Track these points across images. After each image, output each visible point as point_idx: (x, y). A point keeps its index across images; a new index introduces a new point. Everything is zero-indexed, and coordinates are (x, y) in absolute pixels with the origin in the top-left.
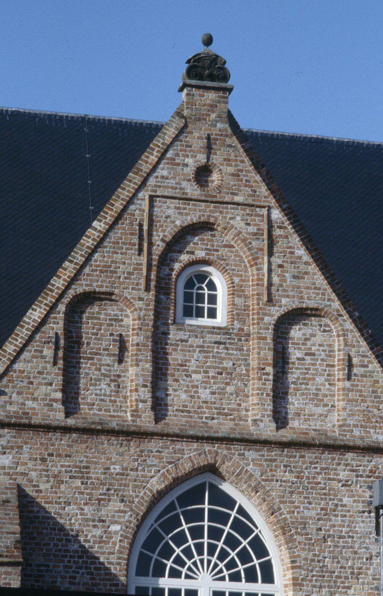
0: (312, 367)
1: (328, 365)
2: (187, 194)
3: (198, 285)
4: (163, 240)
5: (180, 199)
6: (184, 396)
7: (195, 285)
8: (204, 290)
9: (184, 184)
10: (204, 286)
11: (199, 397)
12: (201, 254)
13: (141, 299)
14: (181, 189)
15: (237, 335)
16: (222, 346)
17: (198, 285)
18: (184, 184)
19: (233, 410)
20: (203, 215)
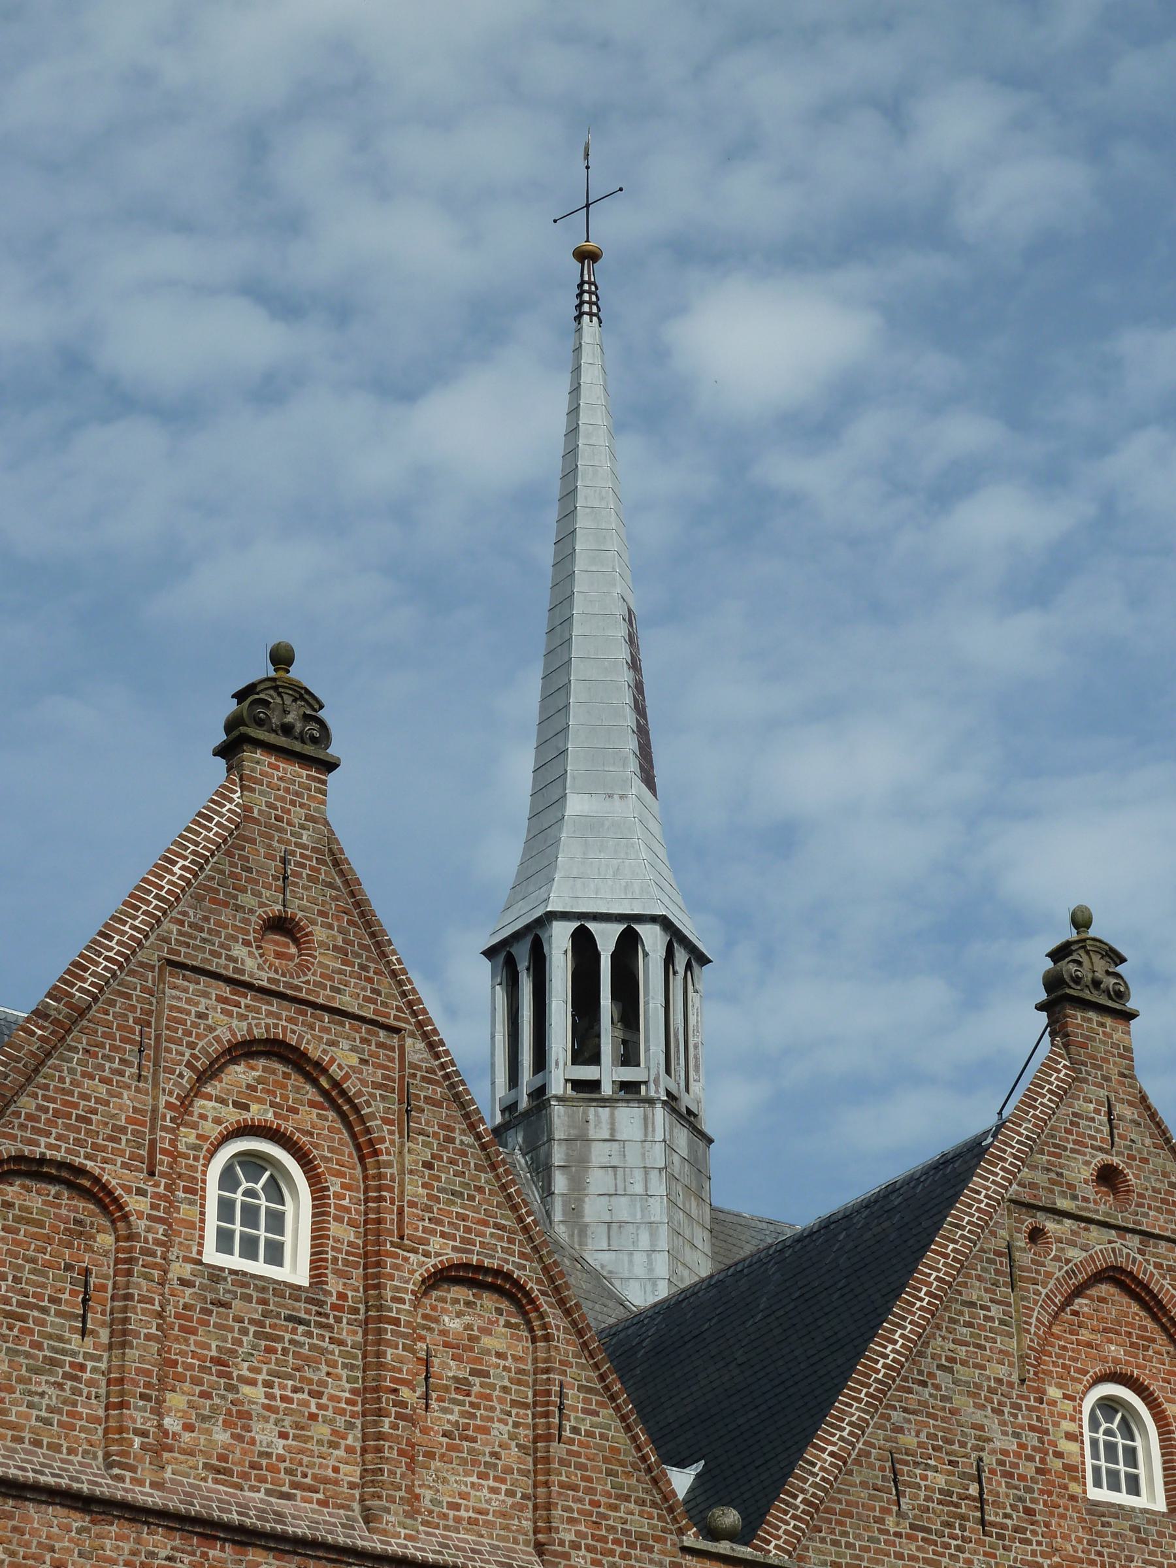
0: (483, 1403)
1: (514, 1403)
2: (242, 972)
3: (245, 1185)
4: (189, 1065)
5: (229, 981)
6: (222, 1437)
7: (239, 1184)
8: (258, 1198)
9: (239, 951)
10: (259, 1187)
11: (253, 1442)
12: (259, 1113)
13: (141, 1192)
14: (230, 958)
15: (334, 1307)
16: (301, 1328)
17: (245, 1185)
18: (239, 951)
19: (326, 1481)
20: (276, 1026)
